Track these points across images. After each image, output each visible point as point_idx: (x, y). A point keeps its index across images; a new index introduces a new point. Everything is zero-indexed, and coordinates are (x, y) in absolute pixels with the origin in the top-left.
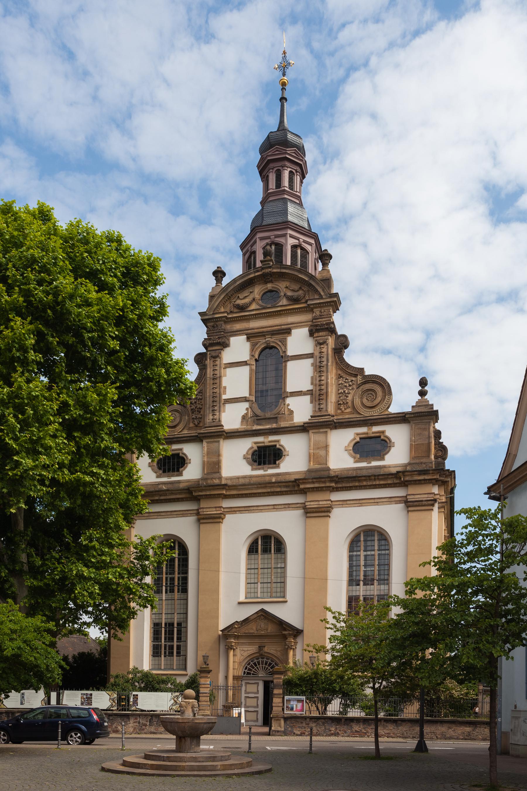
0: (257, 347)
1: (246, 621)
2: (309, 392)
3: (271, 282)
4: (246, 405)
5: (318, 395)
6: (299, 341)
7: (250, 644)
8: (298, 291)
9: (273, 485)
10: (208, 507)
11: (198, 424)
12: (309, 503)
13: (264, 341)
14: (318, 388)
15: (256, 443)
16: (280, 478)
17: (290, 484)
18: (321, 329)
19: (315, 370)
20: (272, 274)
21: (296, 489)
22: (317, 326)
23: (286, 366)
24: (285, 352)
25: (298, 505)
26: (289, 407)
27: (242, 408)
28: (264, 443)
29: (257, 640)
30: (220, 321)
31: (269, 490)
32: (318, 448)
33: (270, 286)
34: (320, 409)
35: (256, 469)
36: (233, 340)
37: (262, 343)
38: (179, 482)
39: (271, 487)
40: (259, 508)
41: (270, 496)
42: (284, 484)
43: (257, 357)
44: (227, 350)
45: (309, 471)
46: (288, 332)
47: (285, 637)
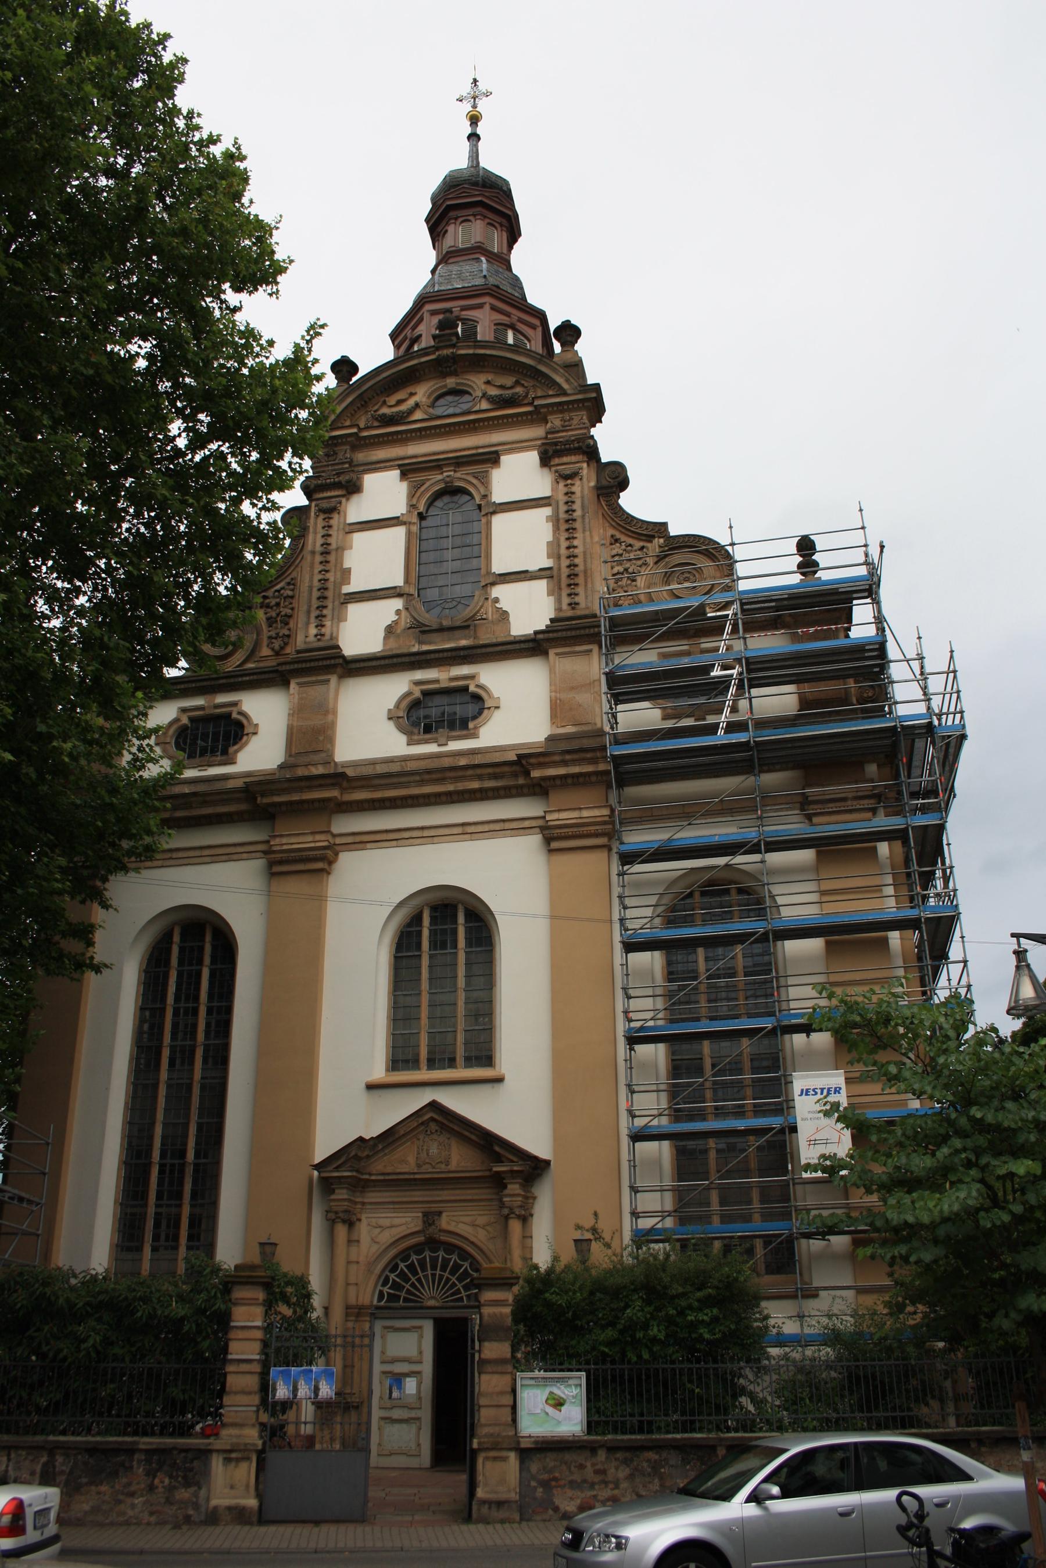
0: (422, 489)
1: (390, 1137)
2: (543, 573)
3: (455, 374)
4: (398, 604)
5: (564, 575)
6: (519, 474)
7: (397, 1206)
8: (511, 388)
9: (460, 773)
10: (298, 838)
11: (282, 648)
12: (555, 816)
13: (440, 477)
14: (565, 562)
15: (417, 683)
16: (478, 760)
17: (506, 769)
18: (567, 450)
19: (556, 529)
20: (455, 359)
21: (521, 781)
22: (556, 444)
23: (489, 524)
24: (485, 496)
25: (527, 824)
26: (497, 605)
27: (388, 610)
28: (437, 681)
29: (418, 1195)
30: (343, 444)
31: (451, 788)
32: (572, 688)
33: (451, 382)
34: (573, 605)
35: (419, 742)
36: (371, 481)
37: (435, 480)
38: (225, 778)
39: (457, 779)
40: (426, 833)
41: (453, 802)
42: (490, 770)
43: (422, 508)
44: (355, 499)
45: (550, 739)
46: (493, 458)
47: (498, 1182)
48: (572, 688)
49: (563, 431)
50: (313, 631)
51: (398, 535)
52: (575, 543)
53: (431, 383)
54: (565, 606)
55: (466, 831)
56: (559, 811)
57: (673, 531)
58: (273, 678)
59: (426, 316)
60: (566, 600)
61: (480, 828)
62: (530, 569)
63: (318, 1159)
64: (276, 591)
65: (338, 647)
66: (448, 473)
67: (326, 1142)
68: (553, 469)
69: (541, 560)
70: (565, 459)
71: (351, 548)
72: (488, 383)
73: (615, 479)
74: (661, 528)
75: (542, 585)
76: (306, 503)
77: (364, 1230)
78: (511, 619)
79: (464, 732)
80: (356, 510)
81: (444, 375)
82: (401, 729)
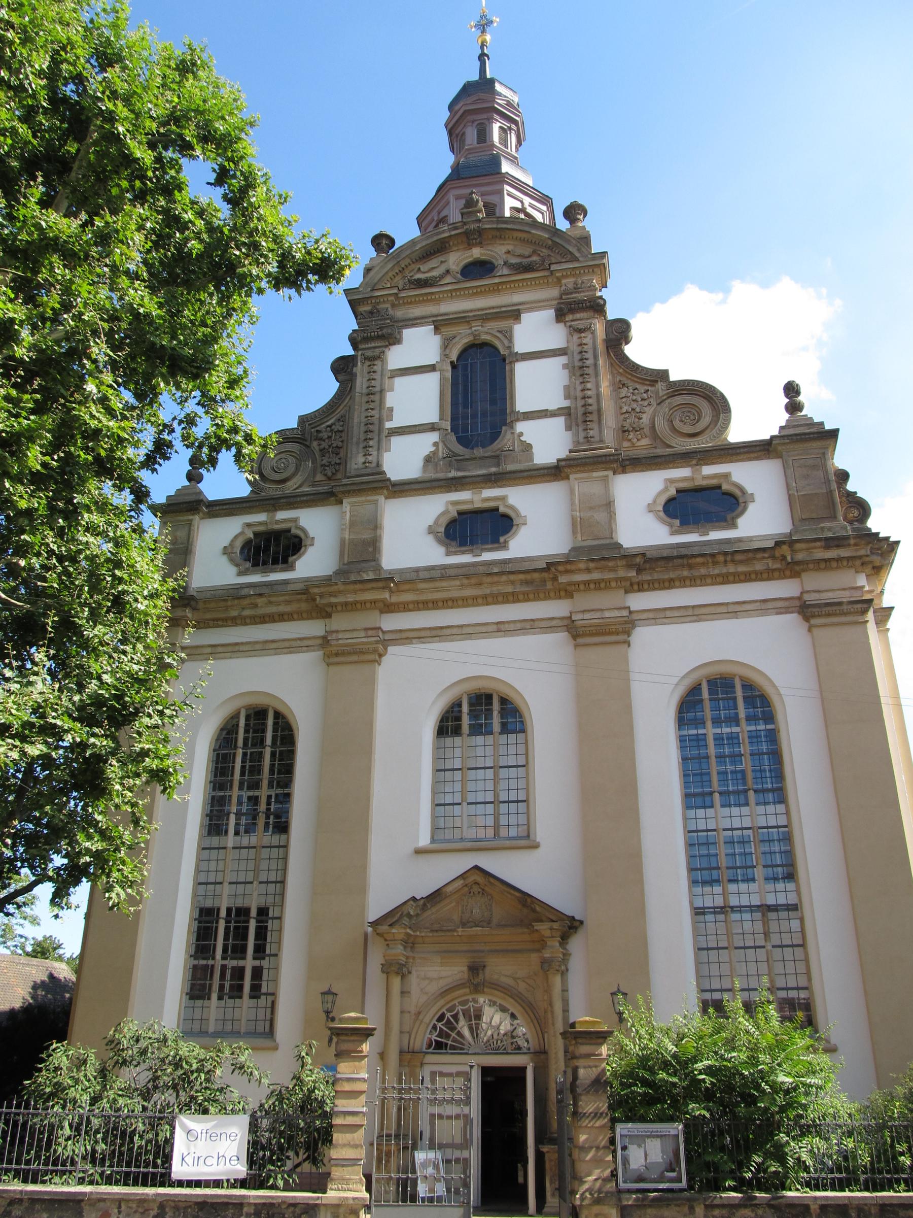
1: (436, 896)
3: (480, 244)
4: (434, 437)
5: (580, 414)
6: (536, 330)
8: (529, 256)
9: (496, 579)
12: (580, 616)
13: (469, 331)
14: (580, 403)
17: (536, 575)
25: (554, 623)
27: (426, 443)
32: (591, 508)
42: (522, 576)
45: (573, 549)
46: (515, 315)
48: (591, 508)
49: (576, 293)
50: (361, 459)
51: (432, 381)
52: (589, 386)
53: (459, 254)
54: (581, 440)
55: (500, 629)
56: (584, 611)
57: (673, 377)
58: (327, 496)
59: (452, 199)
60: (582, 435)
61: (512, 627)
62: (550, 408)
63: (372, 918)
64: (328, 426)
65: (384, 473)
66: (476, 327)
67: (378, 904)
68: (568, 324)
69: (557, 401)
70: (578, 316)
71: (393, 390)
72: (508, 252)
73: (620, 332)
74: (664, 374)
75: (560, 421)
76: (353, 353)
77: (414, 981)
78: (534, 450)
79: (496, 545)
80: (396, 357)
81: (470, 246)
82: (439, 541)
